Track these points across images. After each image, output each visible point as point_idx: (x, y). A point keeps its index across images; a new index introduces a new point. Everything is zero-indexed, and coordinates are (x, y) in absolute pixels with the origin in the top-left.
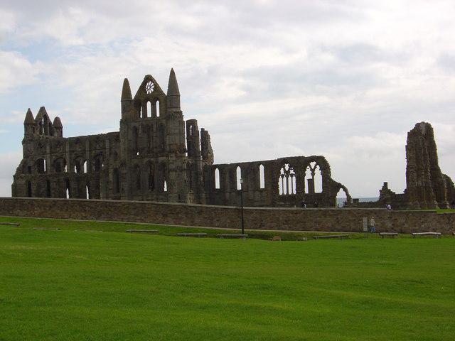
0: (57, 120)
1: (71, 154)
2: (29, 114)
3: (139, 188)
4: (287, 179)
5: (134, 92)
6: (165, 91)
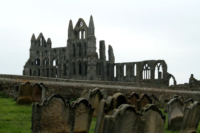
0: (49, 39)
1: (51, 57)
2: (33, 36)
5: (74, 27)
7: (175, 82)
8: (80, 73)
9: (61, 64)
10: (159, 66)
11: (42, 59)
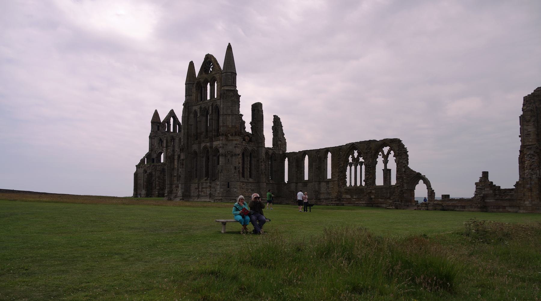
2: (156, 114)
7: (431, 193)
8: (207, 175)
10: (385, 154)
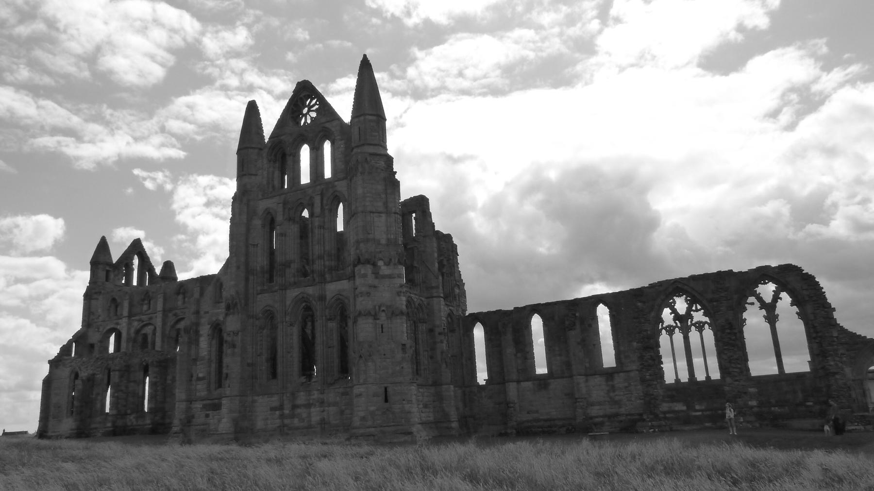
2: (103, 246)
3: (274, 375)
4: (686, 339)
6: (343, 106)
9: (197, 324)
10: (768, 299)
11: (129, 329)
